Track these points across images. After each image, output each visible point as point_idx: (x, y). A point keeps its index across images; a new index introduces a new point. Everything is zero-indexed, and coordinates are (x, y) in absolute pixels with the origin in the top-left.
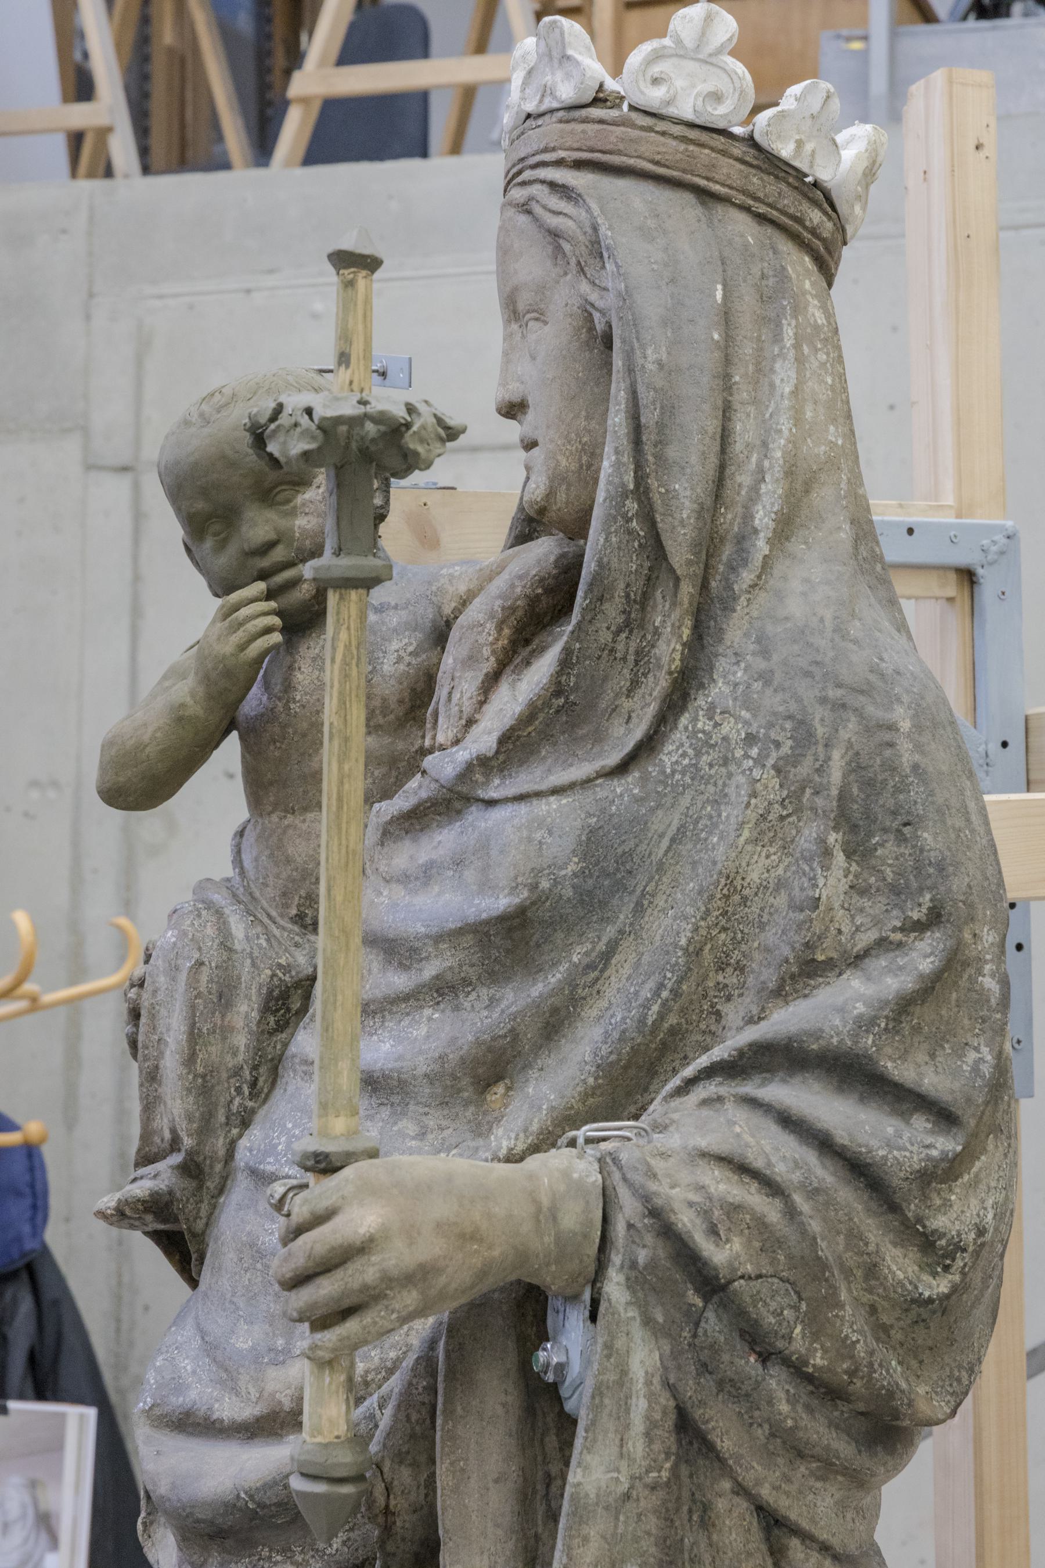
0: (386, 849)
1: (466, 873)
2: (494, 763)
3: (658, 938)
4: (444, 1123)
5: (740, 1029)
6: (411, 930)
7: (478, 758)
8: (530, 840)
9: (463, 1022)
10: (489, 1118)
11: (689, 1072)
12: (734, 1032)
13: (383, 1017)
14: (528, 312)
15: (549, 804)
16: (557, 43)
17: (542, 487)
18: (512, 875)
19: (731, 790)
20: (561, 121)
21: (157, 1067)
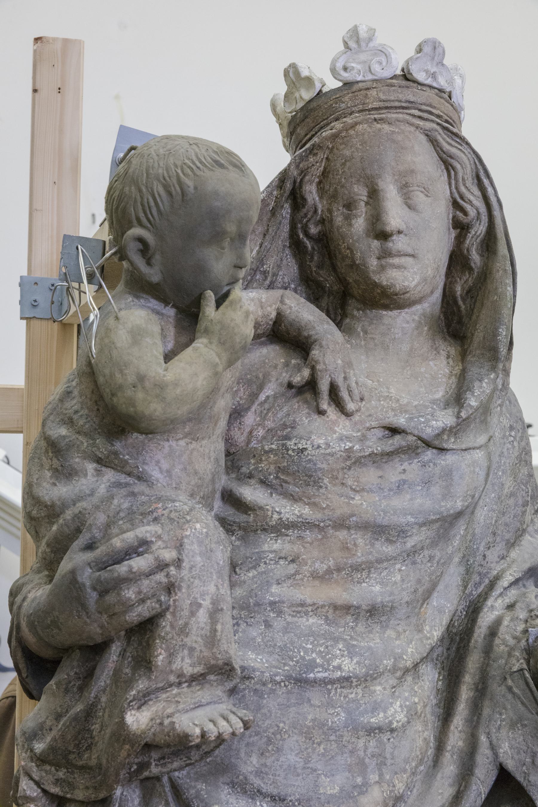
0: (351, 472)
1: (432, 489)
2: (454, 430)
3: (482, 521)
4: (406, 628)
5: (497, 562)
6: (404, 520)
7: (451, 427)
8: (474, 472)
9: (420, 570)
10: (421, 621)
11: (506, 584)
12: (494, 564)
13: (369, 571)
14: (418, 186)
15: (477, 454)
16: (439, 54)
17: (416, 281)
18: (466, 490)
19: (505, 450)
20: (437, 95)
21: (186, 624)
